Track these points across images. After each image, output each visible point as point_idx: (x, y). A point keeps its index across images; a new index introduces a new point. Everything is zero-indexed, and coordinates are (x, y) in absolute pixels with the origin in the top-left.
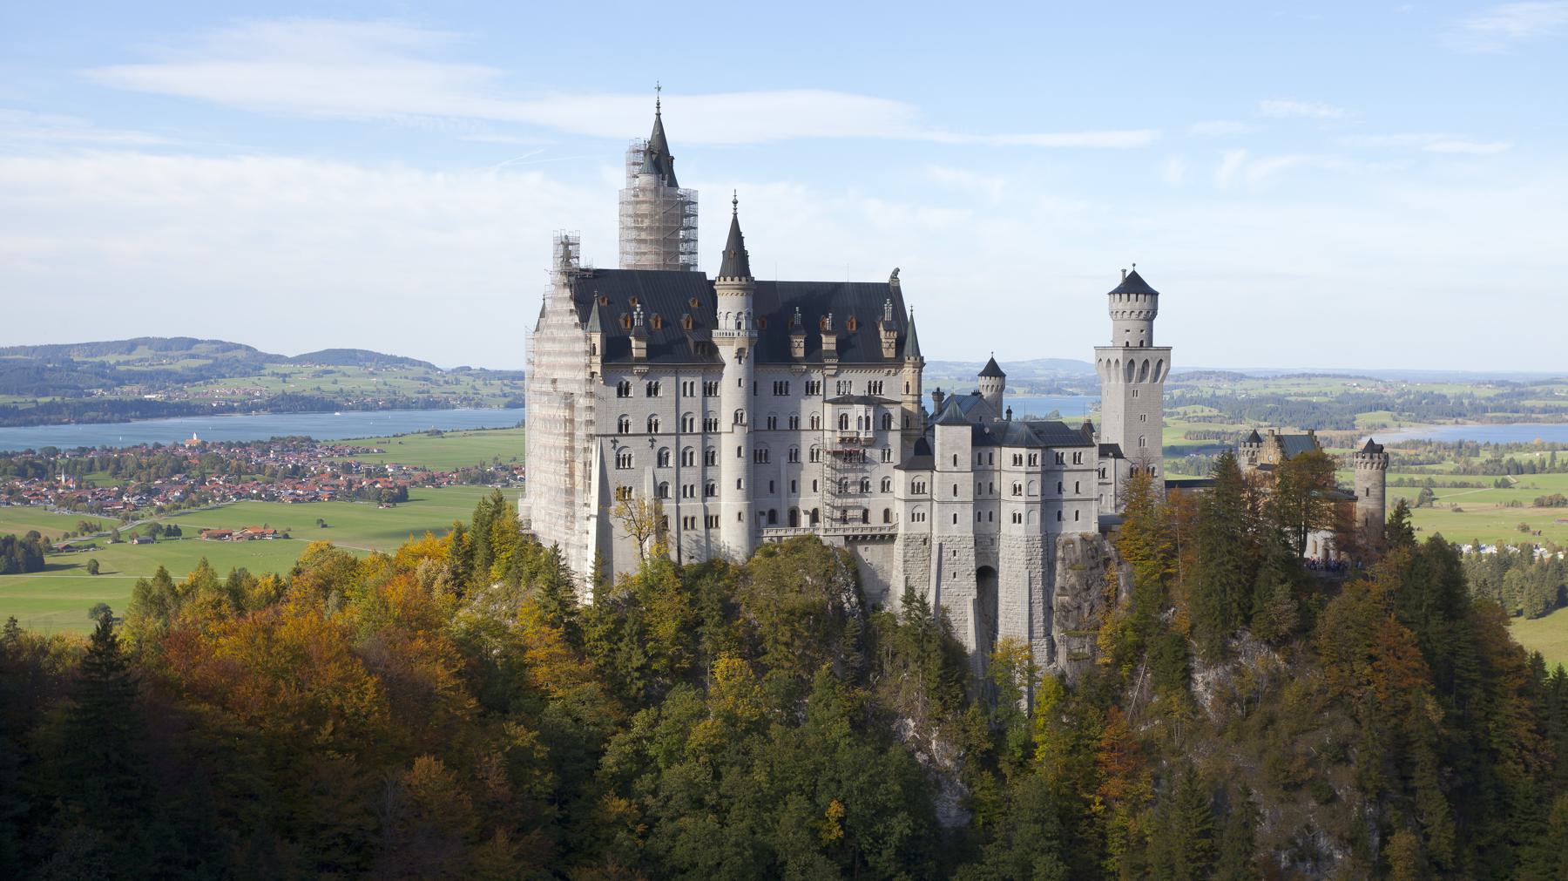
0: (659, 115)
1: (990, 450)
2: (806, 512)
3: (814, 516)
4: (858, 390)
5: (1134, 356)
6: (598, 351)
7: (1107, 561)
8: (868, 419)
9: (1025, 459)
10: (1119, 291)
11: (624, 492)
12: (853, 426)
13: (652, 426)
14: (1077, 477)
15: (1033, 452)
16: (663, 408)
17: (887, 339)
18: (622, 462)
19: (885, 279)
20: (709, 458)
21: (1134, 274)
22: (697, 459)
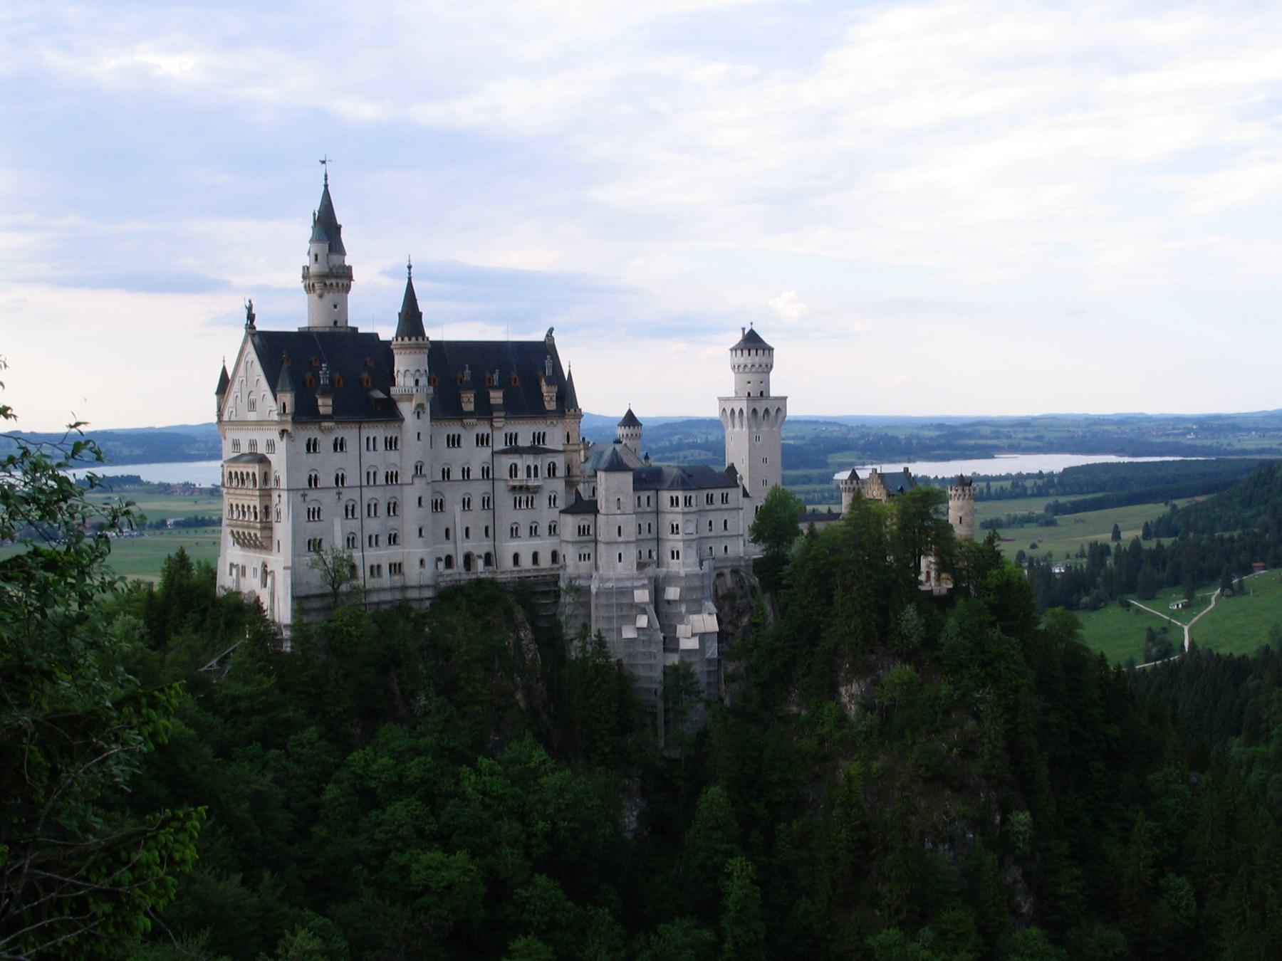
0: (326, 186)
2: (480, 557)
3: (488, 559)
4: (525, 441)
8: (536, 467)
9: (681, 501)
11: (315, 545)
12: (522, 474)
13: (340, 480)
14: (726, 516)
16: (347, 462)
18: (314, 514)
19: (542, 339)
20: (393, 508)
21: (752, 331)
22: (382, 510)
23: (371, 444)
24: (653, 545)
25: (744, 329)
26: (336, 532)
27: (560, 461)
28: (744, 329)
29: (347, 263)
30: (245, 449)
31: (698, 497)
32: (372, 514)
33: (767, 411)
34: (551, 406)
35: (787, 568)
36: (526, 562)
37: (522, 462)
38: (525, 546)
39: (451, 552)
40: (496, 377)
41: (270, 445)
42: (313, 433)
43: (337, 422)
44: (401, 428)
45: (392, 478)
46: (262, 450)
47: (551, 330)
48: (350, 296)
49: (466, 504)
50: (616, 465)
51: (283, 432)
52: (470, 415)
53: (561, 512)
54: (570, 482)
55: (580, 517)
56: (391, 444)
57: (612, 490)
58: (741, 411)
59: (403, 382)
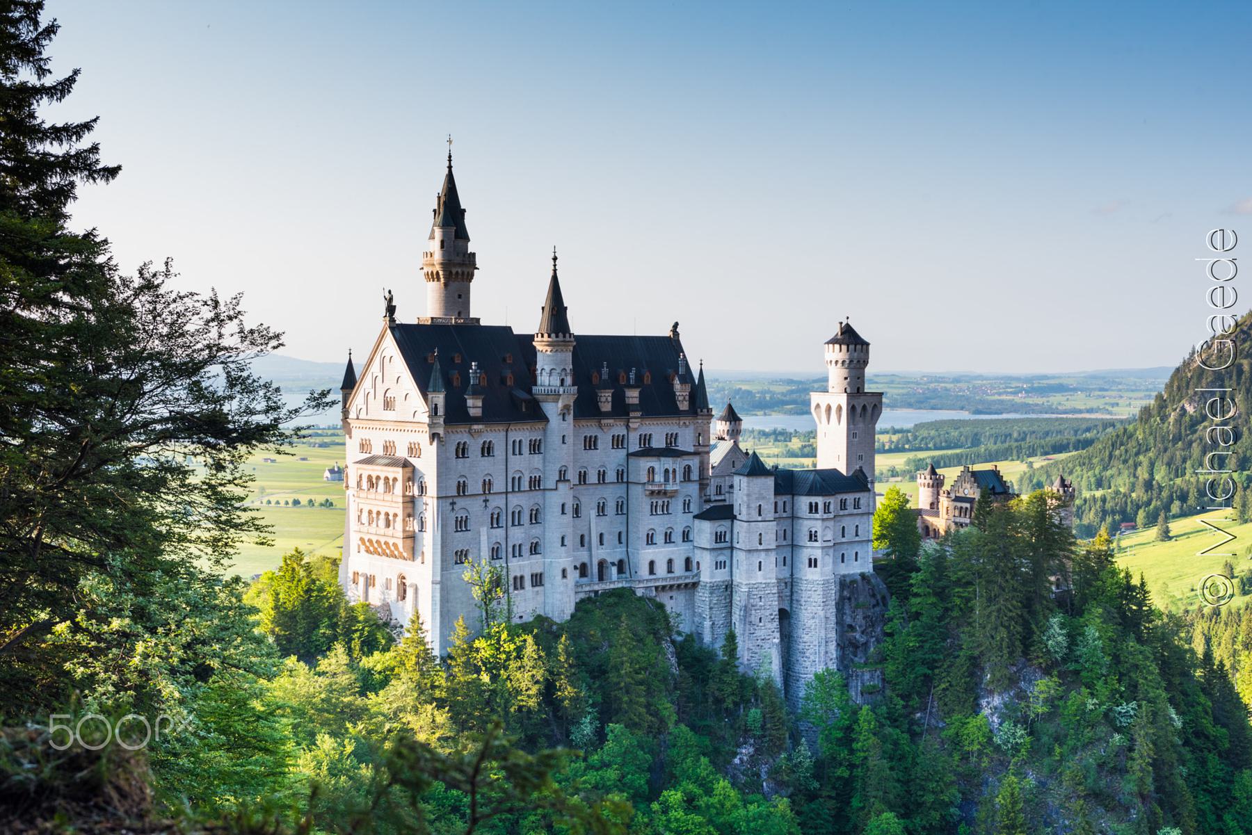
0: (450, 167)
2: (613, 564)
3: (621, 566)
4: (658, 442)
6: (441, 411)
7: (884, 598)
8: (674, 471)
9: (821, 507)
10: (834, 341)
12: (659, 478)
13: (487, 485)
14: (857, 521)
15: (828, 499)
16: (492, 468)
18: (462, 524)
19: (667, 333)
22: (525, 518)
23: (517, 448)
30: (378, 450)
31: (834, 501)
33: (864, 407)
35: (920, 576)
36: (661, 570)
37: (660, 465)
39: (586, 560)
40: (632, 375)
41: (414, 449)
44: (545, 430)
45: (535, 483)
46: (402, 453)
47: (676, 325)
48: (474, 285)
49: (601, 510)
51: (434, 436)
53: (695, 517)
54: (703, 485)
55: (717, 523)
56: (535, 447)
58: (840, 408)
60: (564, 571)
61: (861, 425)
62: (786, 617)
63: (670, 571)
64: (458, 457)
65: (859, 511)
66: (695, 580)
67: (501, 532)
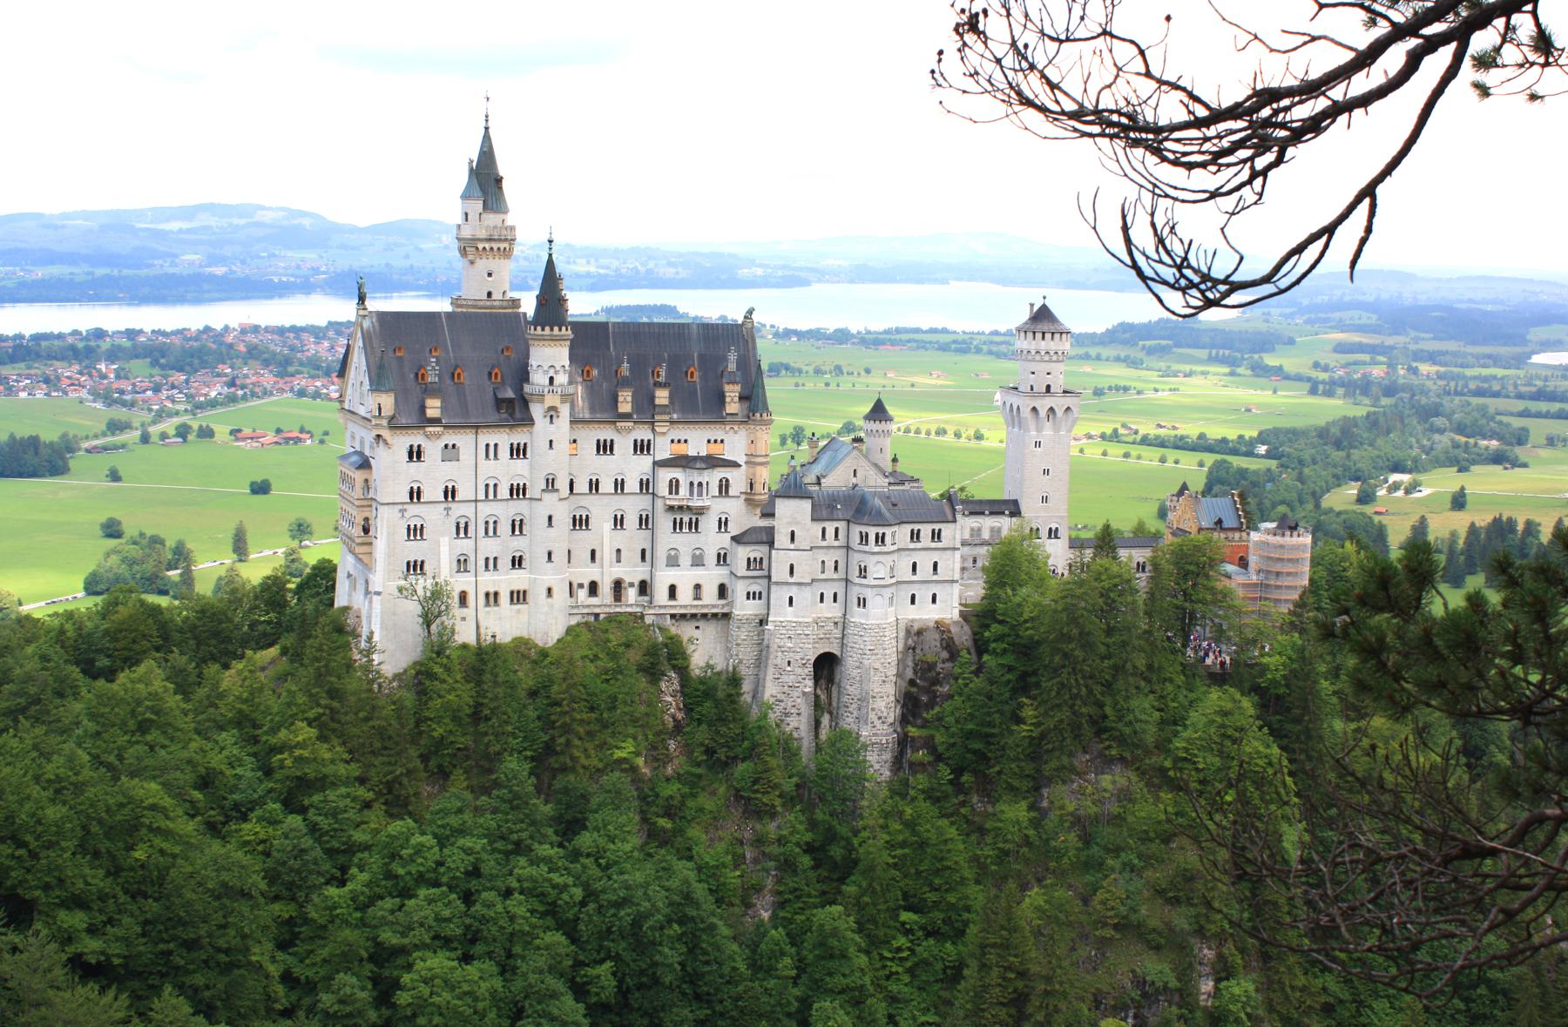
0: (487, 129)
1: (836, 524)
2: (631, 585)
3: (644, 588)
5: (1037, 403)
8: (700, 484)
9: (872, 538)
11: (416, 567)
12: (684, 491)
13: (450, 493)
14: (935, 557)
15: (881, 530)
17: (732, 392)
20: (517, 527)
21: (1044, 309)
23: (492, 452)
24: (839, 588)
25: (1032, 305)
26: (442, 551)
27: (738, 480)
28: (1032, 305)
29: (509, 222)
32: (491, 533)
33: (1051, 409)
34: (733, 406)
38: (684, 578)
42: (416, 439)
43: (445, 427)
45: (518, 491)
47: (751, 312)
49: (619, 522)
50: (792, 488)
52: (626, 416)
53: (733, 538)
56: (518, 451)
57: (792, 514)
59: (538, 379)
60: (549, 590)
61: (1048, 431)
62: (826, 666)
63: (697, 597)
64: (411, 457)
65: (939, 545)
66: (725, 610)
67: (470, 543)
